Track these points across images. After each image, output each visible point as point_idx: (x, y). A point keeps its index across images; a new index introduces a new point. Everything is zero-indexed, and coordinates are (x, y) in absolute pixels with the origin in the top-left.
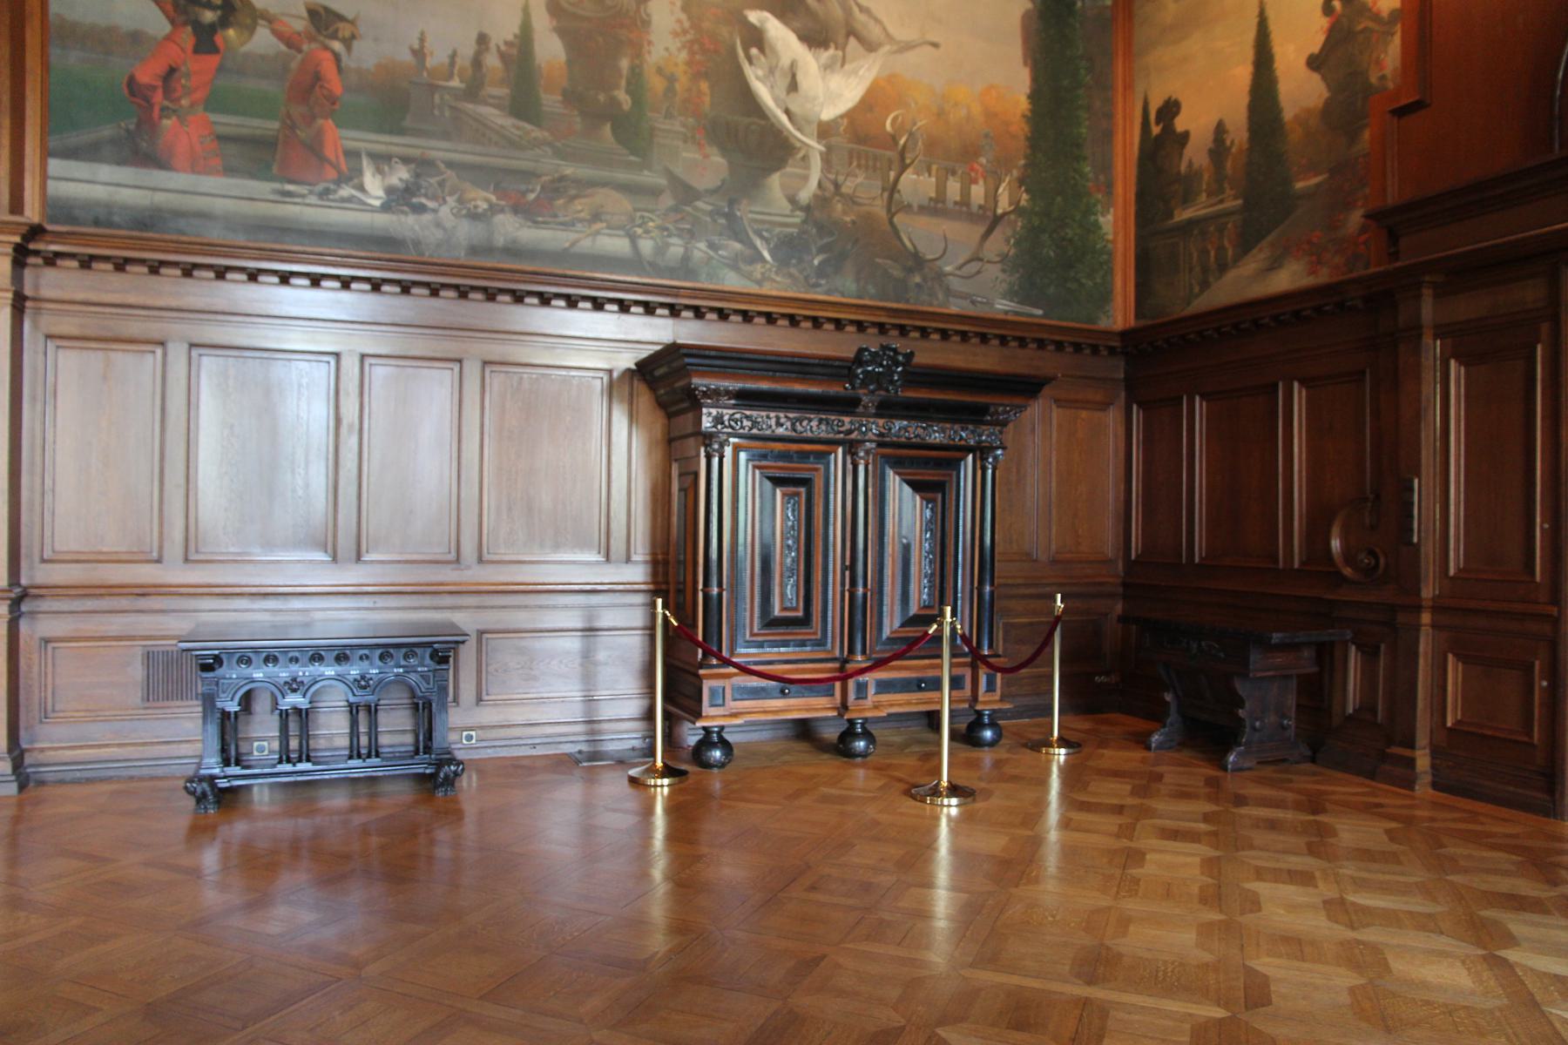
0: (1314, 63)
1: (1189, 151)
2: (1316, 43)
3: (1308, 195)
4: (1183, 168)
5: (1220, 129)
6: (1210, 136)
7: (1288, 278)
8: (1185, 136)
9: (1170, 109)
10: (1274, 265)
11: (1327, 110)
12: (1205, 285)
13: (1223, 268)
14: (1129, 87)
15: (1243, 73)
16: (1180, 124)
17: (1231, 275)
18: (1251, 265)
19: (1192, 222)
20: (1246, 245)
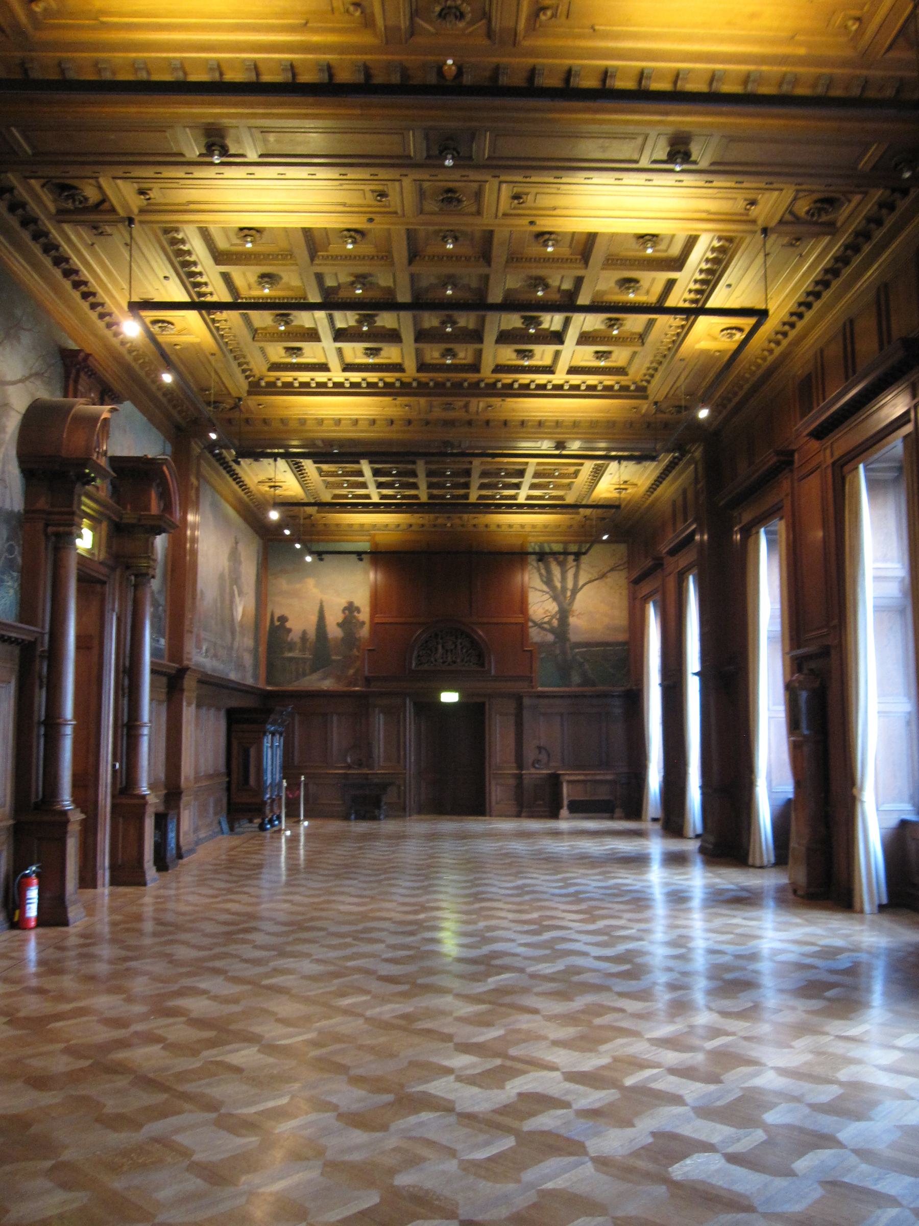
0: (339, 625)
1: (291, 636)
2: (340, 620)
3: (334, 661)
4: (289, 639)
5: (304, 633)
6: (300, 635)
7: (327, 684)
8: (289, 631)
9: (283, 619)
10: (324, 678)
11: (343, 639)
12: (297, 678)
13: (304, 675)
14: (266, 605)
15: (314, 619)
16: (288, 625)
17: (308, 678)
18: (315, 676)
19: (291, 659)
20: (314, 670)
